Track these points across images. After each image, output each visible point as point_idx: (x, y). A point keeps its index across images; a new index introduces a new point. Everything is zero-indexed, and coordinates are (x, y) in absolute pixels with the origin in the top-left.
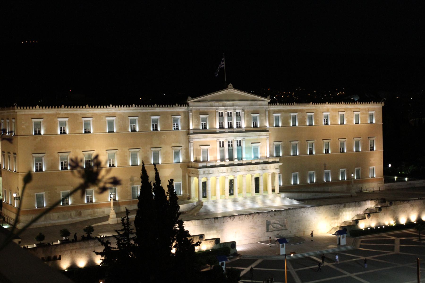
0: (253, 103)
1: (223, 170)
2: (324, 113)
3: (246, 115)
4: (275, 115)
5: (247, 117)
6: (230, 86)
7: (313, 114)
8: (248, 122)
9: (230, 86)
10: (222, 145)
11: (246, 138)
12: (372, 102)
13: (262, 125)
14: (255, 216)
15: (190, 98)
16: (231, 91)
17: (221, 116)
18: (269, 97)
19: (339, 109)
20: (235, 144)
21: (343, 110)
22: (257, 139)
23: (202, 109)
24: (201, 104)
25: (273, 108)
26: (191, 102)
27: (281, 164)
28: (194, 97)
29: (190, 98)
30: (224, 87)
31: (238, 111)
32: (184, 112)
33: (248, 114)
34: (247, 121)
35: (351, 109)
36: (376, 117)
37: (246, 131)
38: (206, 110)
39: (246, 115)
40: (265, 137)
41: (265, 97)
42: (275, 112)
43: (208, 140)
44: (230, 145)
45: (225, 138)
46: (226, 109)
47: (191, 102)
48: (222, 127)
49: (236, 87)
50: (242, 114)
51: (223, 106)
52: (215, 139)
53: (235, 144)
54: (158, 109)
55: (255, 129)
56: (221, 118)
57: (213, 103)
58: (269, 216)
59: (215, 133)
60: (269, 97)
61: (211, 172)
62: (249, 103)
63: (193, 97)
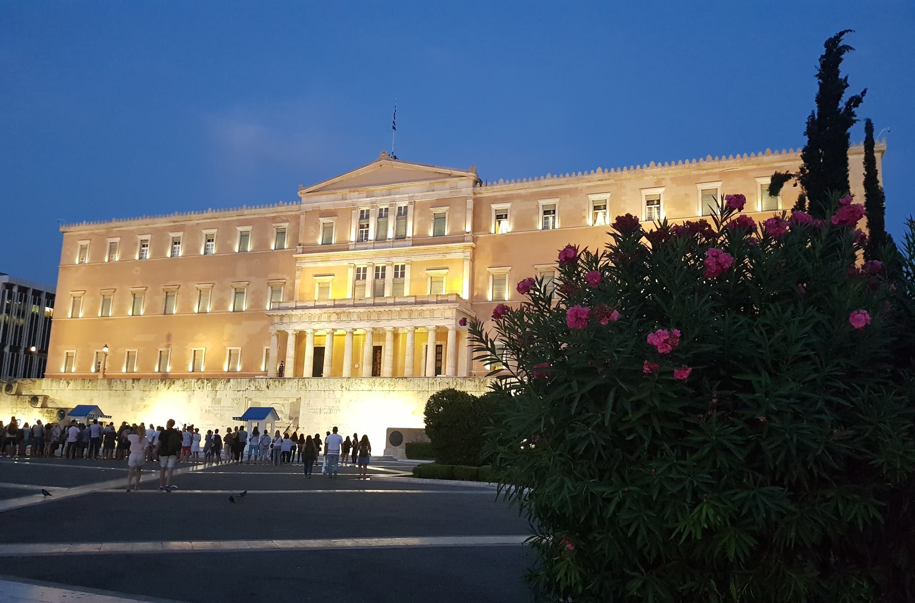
2: (645, 192)
3: (417, 212)
4: (495, 207)
5: (420, 215)
8: (422, 227)
10: (360, 274)
13: (456, 231)
14: (220, 386)
17: (365, 216)
20: (390, 273)
22: (442, 261)
34: (419, 223)
35: (743, 172)
39: (417, 212)
40: (460, 256)
42: (496, 200)
44: (380, 273)
48: (362, 238)
52: (345, 263)
53: (390, 273)
54: (249, 213)
55: (439, 238)
58: (253, 388)
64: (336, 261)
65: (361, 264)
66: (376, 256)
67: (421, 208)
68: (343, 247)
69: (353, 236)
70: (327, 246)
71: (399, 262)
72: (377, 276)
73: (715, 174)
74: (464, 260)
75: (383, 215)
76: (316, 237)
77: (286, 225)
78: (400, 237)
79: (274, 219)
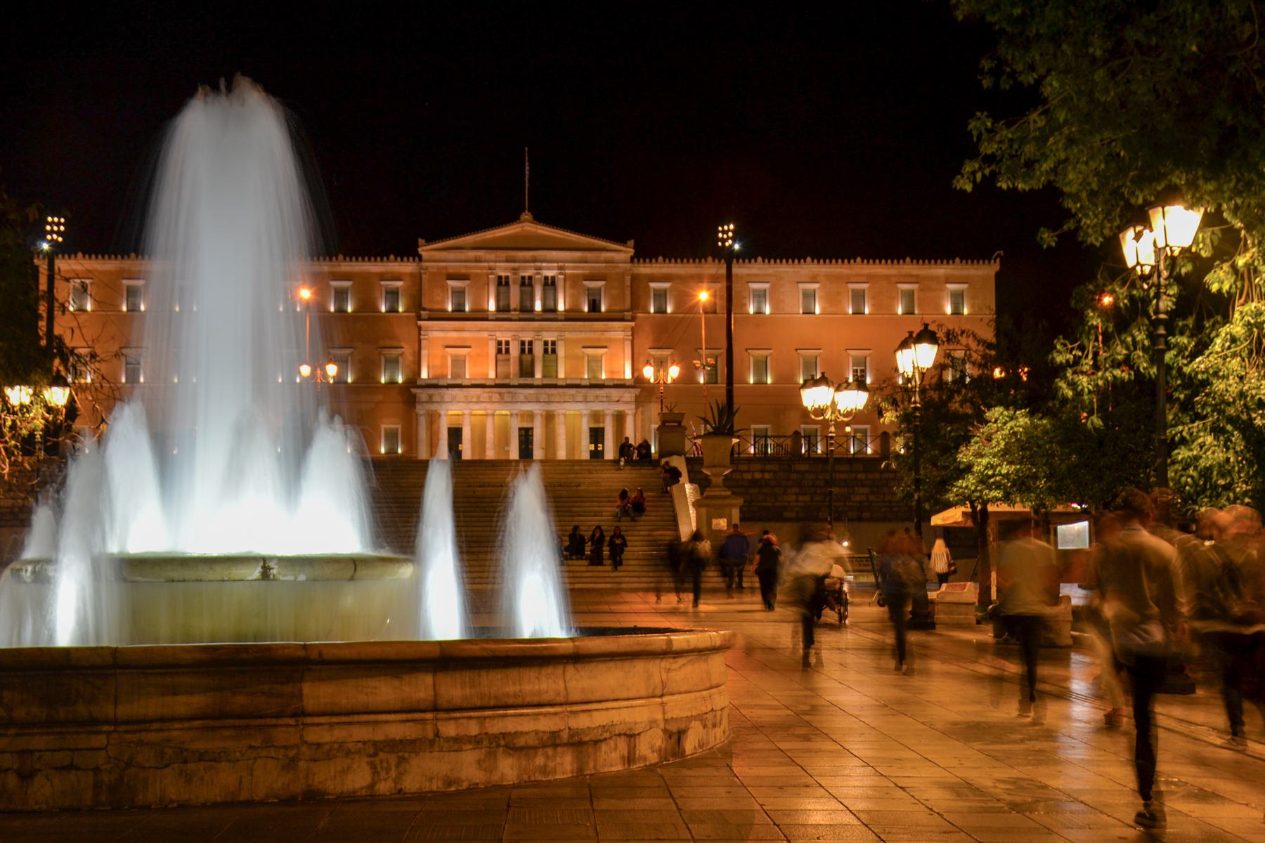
0: (588, 255)
1: (479, 397)
2: (802, 286)
4: (653, 285)
5: (572, 287)
6: (527, 216)
7: (766, 286)
8: (575, 300)
9: (527, 216)
11: (568, 335)
12: (957, 260)
15: (421, 241)
16: (527, 227)
18: (631, 243)
19: (848, 276)
20: (538, 349)
21: (864, 279)
22: (599, 340)
23: (453, 267)
24: (452, 255)
25: (645, 269)
26: (425, 250)
27: (637, 391)
28: (433, 237)
29: (421, 241)
30: (511, 217)
31: (550, 273)
32: (411, 275)
33: (574, 281)
34: (572, 296)
35: (887, 277)
36: (973, 298)
37: (566, 320)
38: (463, 271)
40: (620, 335)
41: (623, 241)
43: (466, 335)
45: (507, 332)
46: (515, 270)
47: (425, 250)
49: (540, 218)
50: (560, 284)
51: (507, 261)
52: (485, 335)
53: (538, 349)
56: (503, 289)
57: (480, 253)
59: (487, 319)
60: (631, 243)
61: (446, 399)
62: (578, 254)
63: (429, 240)
64: (470, 331)
65: (503, 337)
66: (523, 330)
67: (574, 281)
68: (480, 315)
69: (492, 306)
70: (459, 315)
71: (550, 337)
72: (523, 351)
73: (862, 275)
74: (624, 340)
75: (527, 283)
76: (443, 302)
77: (399, 284)
78: (550, 311)
79: (383, 276)
